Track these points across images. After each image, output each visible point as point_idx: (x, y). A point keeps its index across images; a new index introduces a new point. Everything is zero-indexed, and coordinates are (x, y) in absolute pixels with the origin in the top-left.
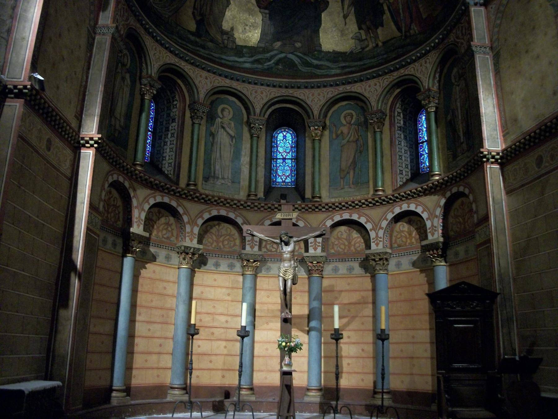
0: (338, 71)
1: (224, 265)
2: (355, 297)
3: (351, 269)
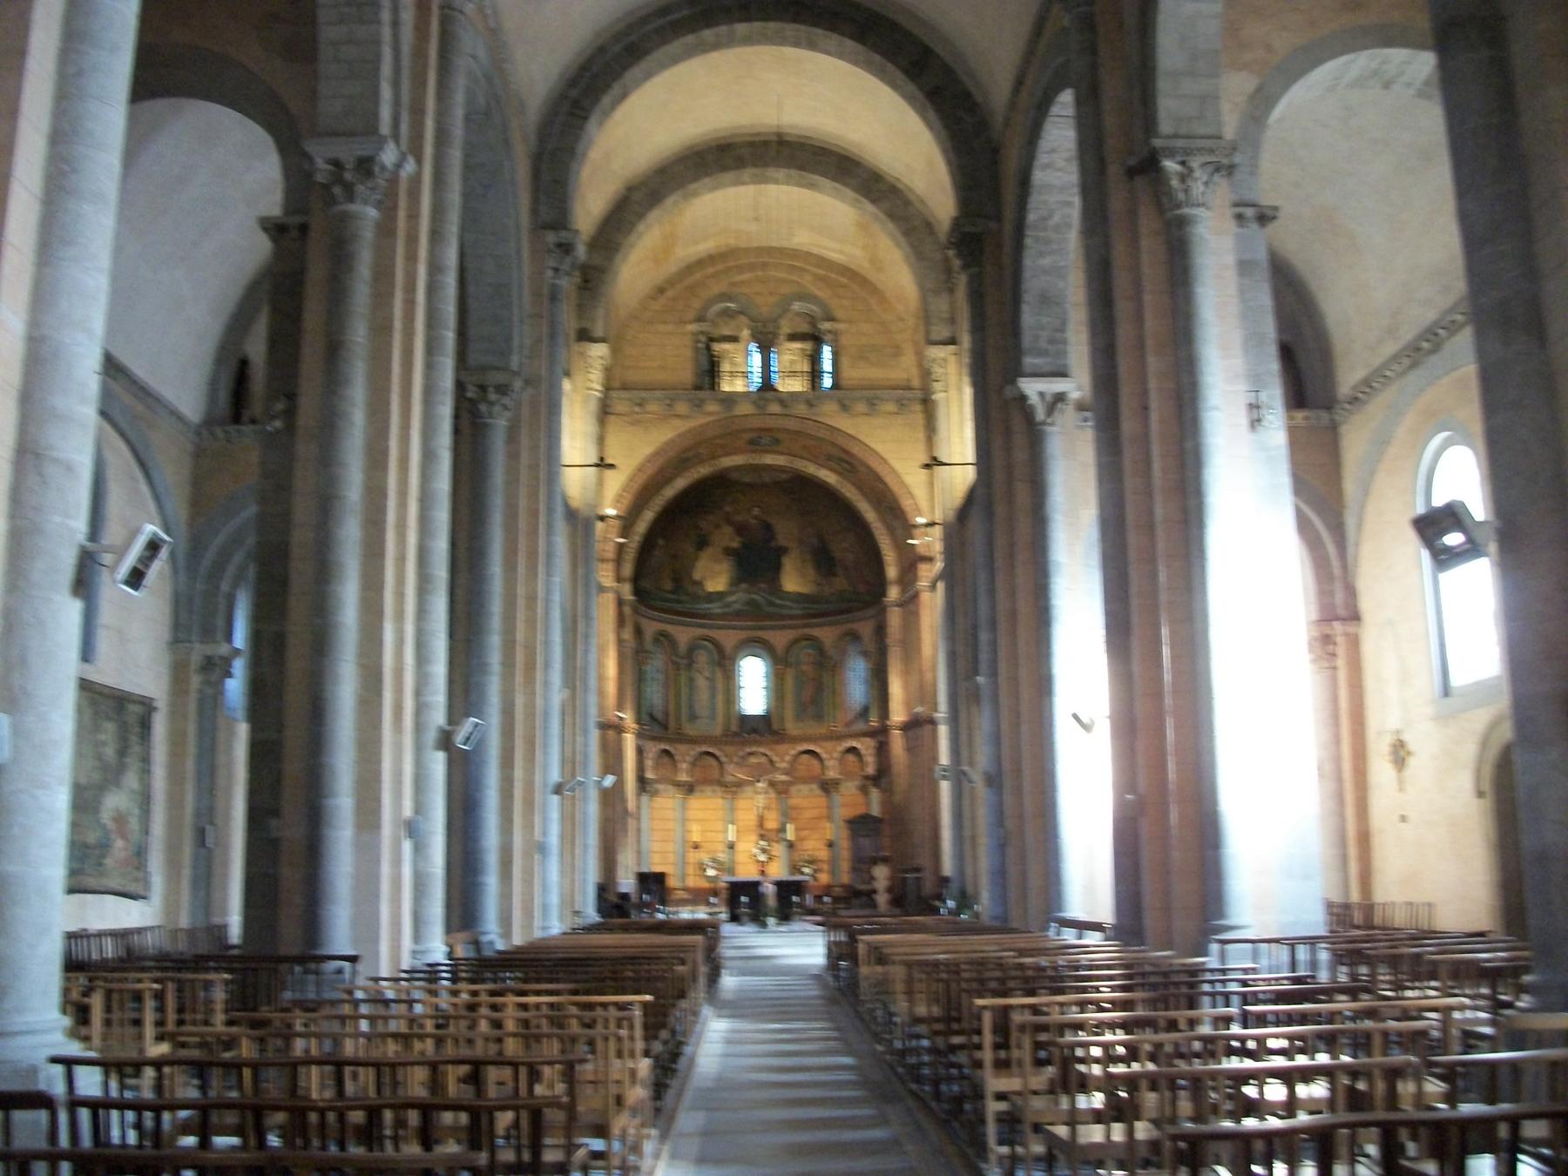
0: (799, 612)
1: (708, 790)
2: (816, 813)
3: (811, 790)
